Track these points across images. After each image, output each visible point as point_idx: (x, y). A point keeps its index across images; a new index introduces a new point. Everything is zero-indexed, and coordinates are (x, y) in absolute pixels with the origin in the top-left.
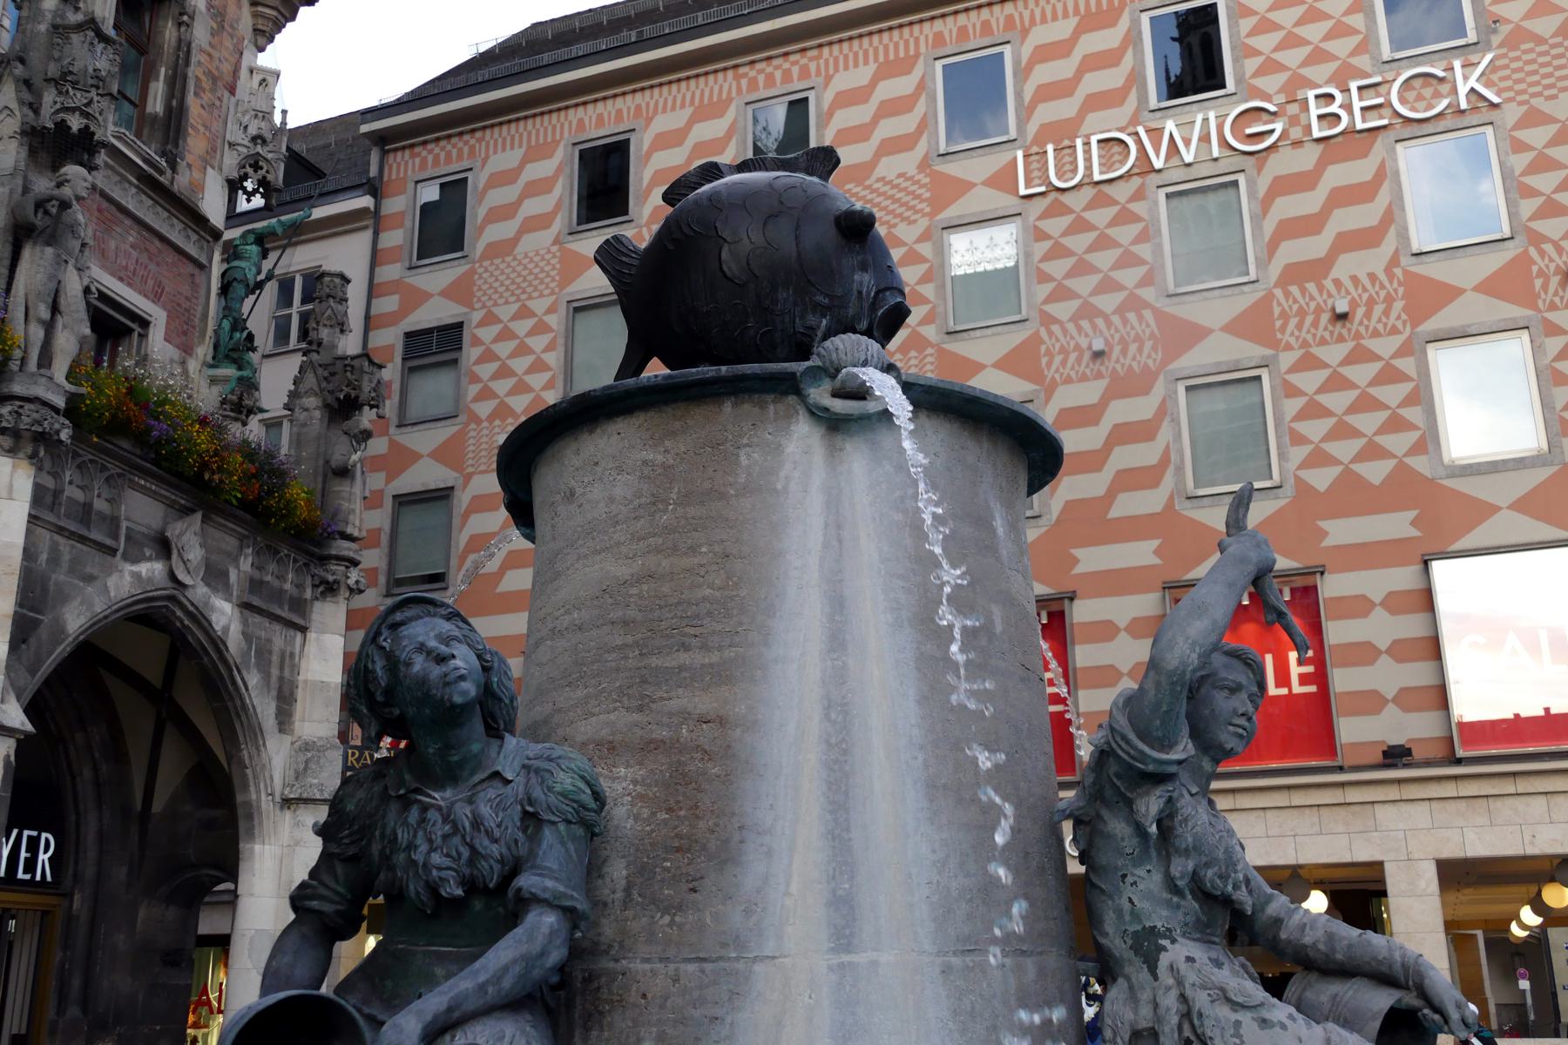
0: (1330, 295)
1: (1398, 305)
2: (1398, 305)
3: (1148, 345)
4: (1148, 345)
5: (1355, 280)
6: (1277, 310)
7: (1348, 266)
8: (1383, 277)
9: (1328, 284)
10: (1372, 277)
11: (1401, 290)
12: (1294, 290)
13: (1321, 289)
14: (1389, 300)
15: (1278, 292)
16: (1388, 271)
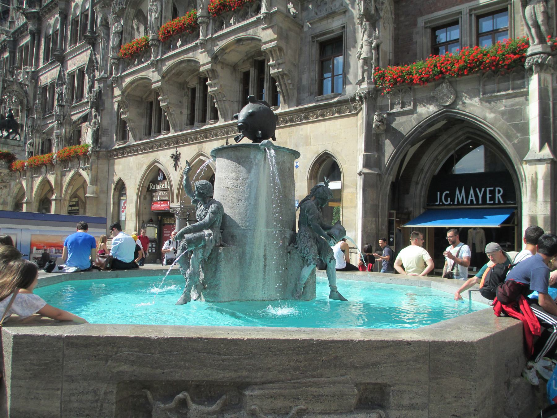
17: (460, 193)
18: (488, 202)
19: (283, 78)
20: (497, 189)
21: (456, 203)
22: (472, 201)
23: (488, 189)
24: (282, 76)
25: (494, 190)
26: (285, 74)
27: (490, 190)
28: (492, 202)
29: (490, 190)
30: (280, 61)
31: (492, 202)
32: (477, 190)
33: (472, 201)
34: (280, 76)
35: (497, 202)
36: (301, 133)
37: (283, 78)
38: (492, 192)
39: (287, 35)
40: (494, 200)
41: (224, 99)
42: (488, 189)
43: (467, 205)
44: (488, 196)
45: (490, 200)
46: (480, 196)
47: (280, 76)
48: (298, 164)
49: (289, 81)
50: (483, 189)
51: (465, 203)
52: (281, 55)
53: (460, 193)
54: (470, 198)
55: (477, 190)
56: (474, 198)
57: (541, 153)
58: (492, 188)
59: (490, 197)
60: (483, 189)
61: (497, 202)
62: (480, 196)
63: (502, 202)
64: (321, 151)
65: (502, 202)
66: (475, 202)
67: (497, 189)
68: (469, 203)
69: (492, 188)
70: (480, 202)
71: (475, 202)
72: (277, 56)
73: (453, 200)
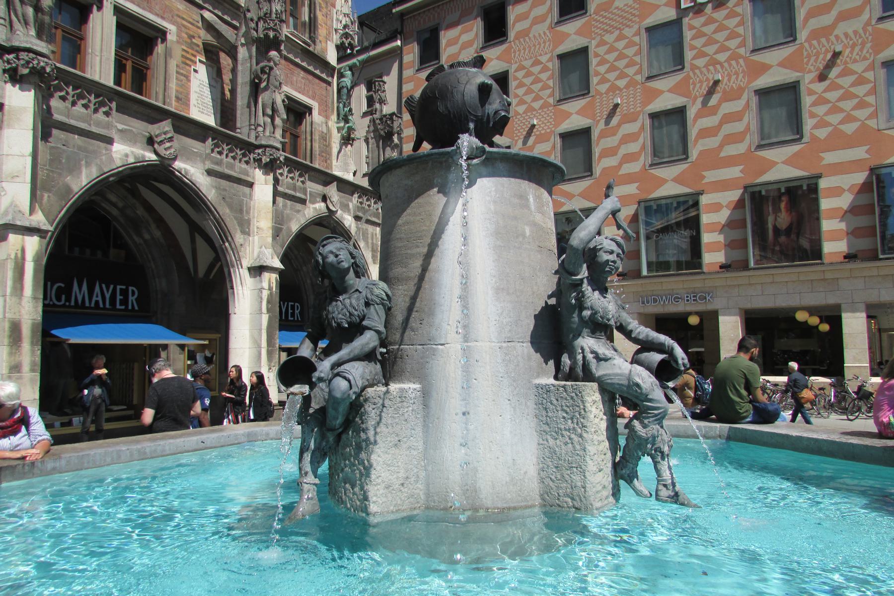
0: (833, 44)
1: (869, 45)
2: (869, 45)
3: (741, 76)
4: (741, 76)
5: (846, 35)
6: (805, 54)
7: (843, 28)
8: (861, 31)
9: (832, 38)
10: (855, 32)
11: (870, 38)
12: (823, 40)
13: (828, 41)
14: (863, 44)
15: (806, 45)
16: (864, 29)
17: (80, 287)
18: (118, 307)
20: (131, 288)
21: (73, 303)
22: (97, 302)
23: (118, 287)
25: (127, 290)
27: (121, 289)
28: (123, 307)
29: (121, 289)
31: (123, 307)
32: (104, 286)
33: (97, 302)
35: (130, 307)
38: (124, 293)
40: (127, 306)
42: (118, 287)
43: (90, 308)
44: (119, 297)
45: (121, 305)
46: (108, 296)
50: (112, 287)
51: (87, 304)
53: (80, 287)
54: (94, 299)
55: (104, 286)
56: (100, 299)
58: (124, 287)
59: (120, 300)
60: (112, 287)
61: (130, 307)
62: (108, 296)
63: (136, 308)
65: (136, 308)
66: (101, 306)
67: (131, 288)
68: (93, 305)
69: (124, 287)
70: (108, 306)
71: (101, 306)
73: (68, 299)
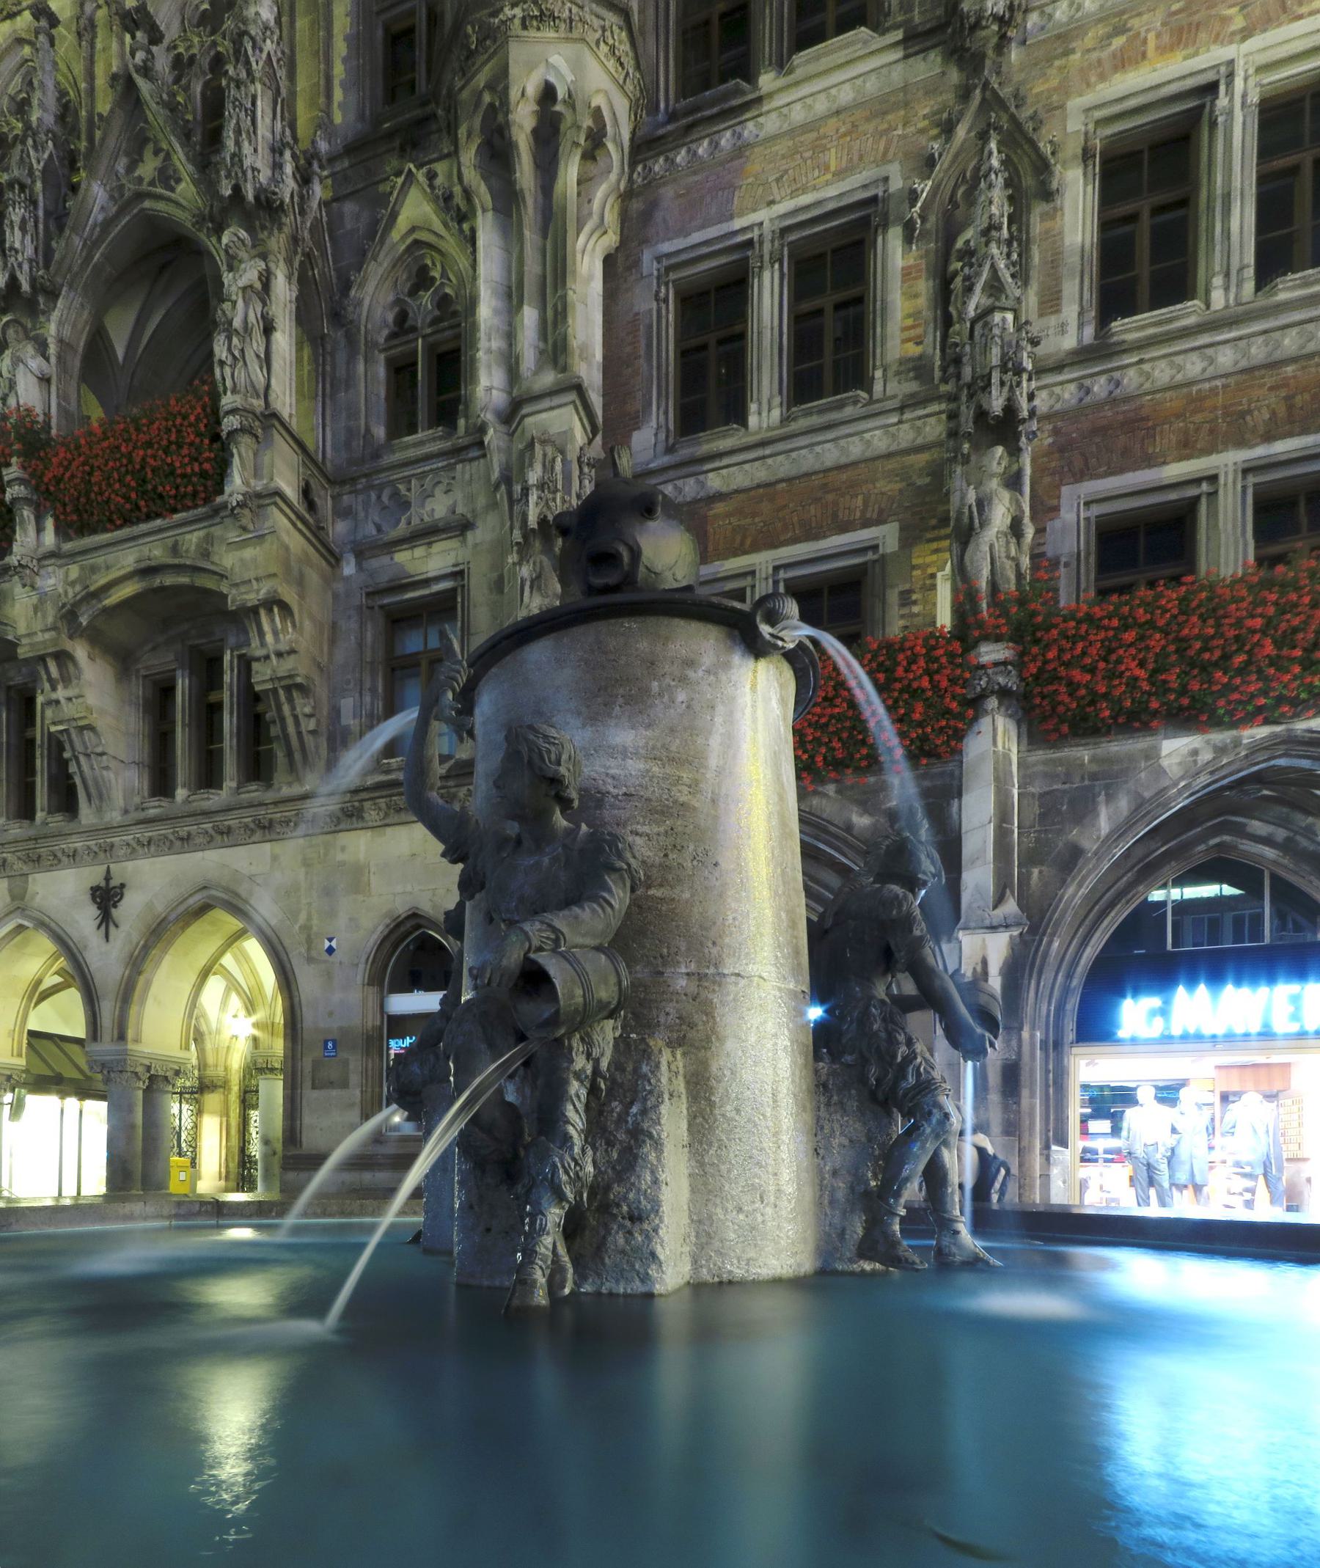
19: (290, 700)
24: (288, 689)
26: (300, 687)
30: (283, 647)
34: (281, 692)
36: (340, 857)
37: (290, 700)
39: (302, 575)
41: (99, 750)
47: (281, 692)
48: (334, 944)
49: (307, 710)
52: (285, 629)
57: (996, 912)
64: (402, 909)
72: (275, 633)
